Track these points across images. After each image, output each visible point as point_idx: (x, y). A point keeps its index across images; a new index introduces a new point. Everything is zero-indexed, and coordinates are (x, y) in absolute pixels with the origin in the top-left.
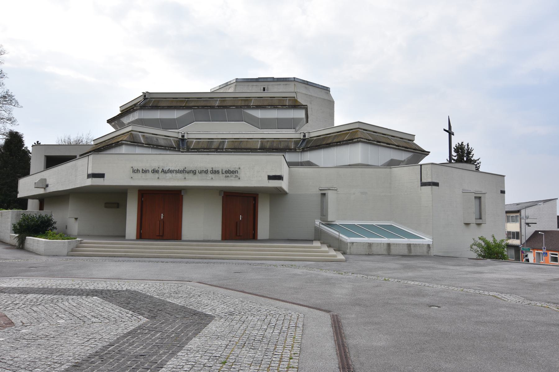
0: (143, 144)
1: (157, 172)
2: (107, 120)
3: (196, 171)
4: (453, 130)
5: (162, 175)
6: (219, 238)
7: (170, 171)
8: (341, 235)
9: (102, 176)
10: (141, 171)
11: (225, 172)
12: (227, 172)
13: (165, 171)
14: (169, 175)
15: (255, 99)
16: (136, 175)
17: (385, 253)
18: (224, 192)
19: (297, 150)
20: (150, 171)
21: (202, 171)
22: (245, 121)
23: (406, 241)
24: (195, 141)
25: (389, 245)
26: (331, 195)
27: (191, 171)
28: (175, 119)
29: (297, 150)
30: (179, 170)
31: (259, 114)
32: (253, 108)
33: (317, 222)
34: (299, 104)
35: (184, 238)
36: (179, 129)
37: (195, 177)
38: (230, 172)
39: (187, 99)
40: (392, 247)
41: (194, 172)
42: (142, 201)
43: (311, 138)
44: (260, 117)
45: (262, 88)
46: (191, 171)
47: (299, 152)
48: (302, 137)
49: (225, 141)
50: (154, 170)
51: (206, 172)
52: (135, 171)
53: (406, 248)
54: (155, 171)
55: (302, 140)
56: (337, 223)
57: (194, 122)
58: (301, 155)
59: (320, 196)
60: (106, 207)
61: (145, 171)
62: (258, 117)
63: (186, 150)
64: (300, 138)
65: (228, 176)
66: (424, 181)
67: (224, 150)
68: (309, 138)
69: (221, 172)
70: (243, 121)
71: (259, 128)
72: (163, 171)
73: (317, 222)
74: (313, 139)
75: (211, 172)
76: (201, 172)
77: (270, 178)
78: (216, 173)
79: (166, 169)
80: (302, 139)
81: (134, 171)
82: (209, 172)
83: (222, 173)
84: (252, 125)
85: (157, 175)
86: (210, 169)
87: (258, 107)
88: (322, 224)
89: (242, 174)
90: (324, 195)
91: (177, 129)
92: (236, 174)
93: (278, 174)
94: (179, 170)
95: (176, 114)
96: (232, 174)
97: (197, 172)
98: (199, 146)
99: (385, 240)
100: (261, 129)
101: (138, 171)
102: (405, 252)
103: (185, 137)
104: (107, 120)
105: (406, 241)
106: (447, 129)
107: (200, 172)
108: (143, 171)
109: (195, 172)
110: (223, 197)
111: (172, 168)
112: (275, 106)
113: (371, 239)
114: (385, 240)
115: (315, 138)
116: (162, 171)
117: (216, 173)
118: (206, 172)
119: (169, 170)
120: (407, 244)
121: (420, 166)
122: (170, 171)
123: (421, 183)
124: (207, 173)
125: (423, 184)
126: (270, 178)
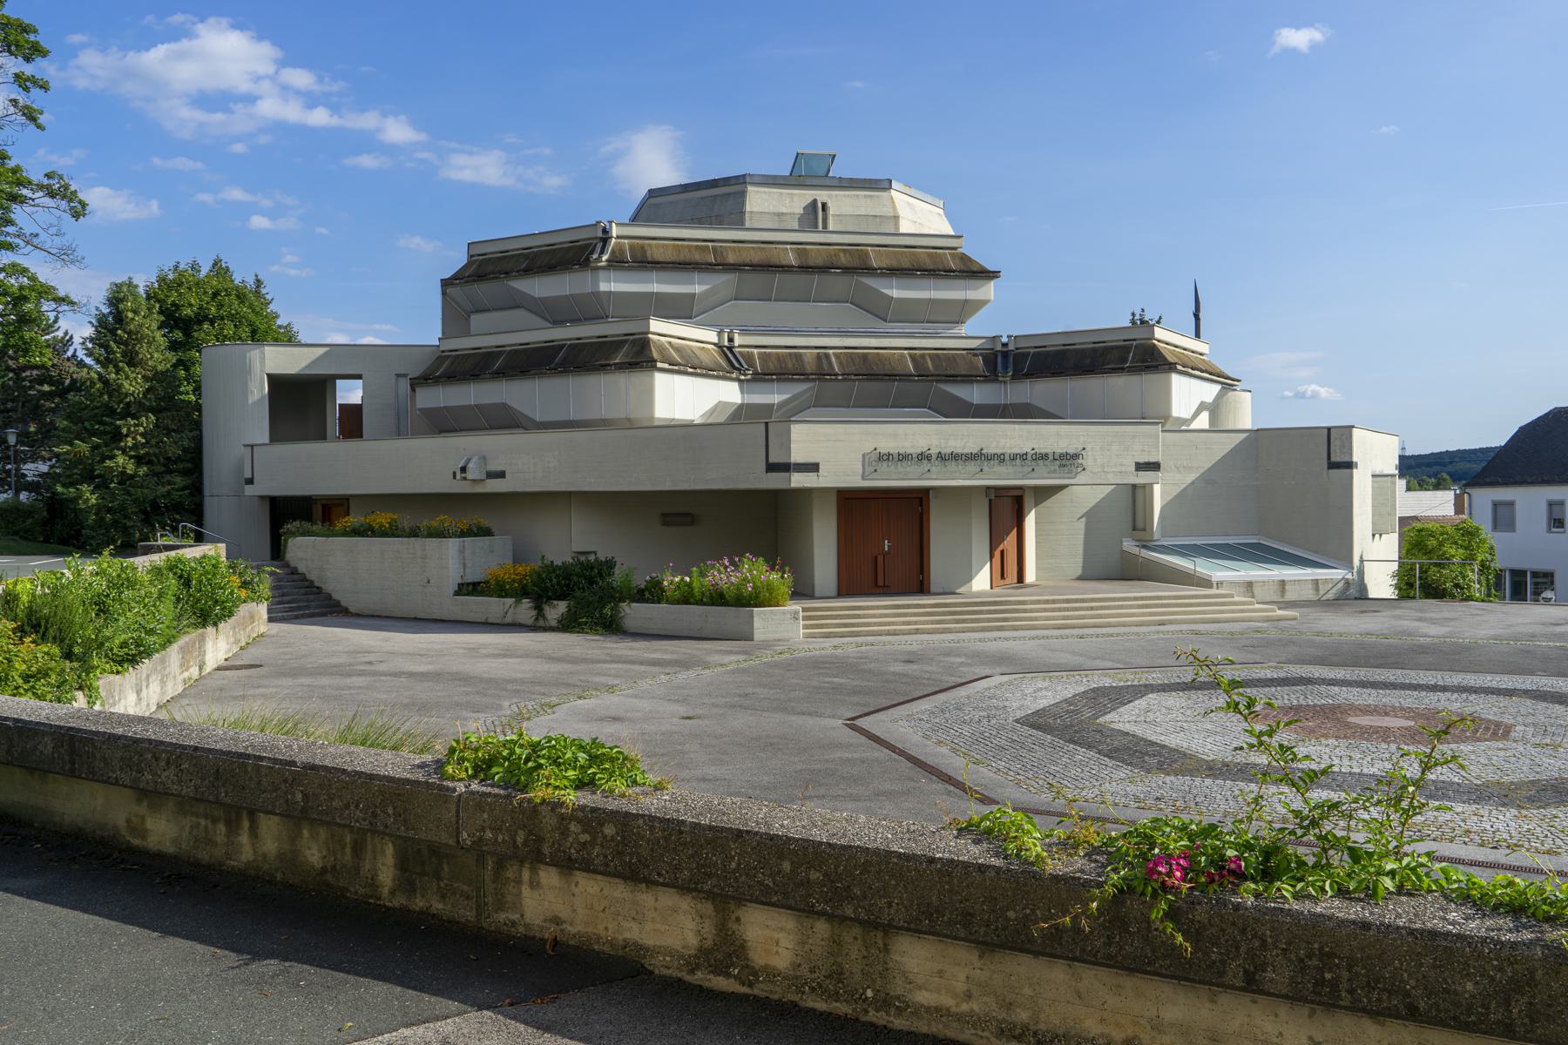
0: (679, 364)
1: (929, 458)
2: (442, 280)
5: (936, 468)
10: (896, 456)
14: (952, 466)
15: (875, 251)
16: (884, 467)
19: (1001, 379)
24: (759, 354)
25: (1283, 583)
29: (1001, 379)
32: (882, 275)
33: (1129, 545)
35: (933, 589)
37: (1002, 469)
39: (710, 244)
40: (1287, 587)
43: (1017, 349)
49: (827, 356)
52: (884, 458)
53: (1310, 586)
56: (1165, 543)
60: (665, 524)
63: (749, 377)
67: (840, 377)
69: (1051, 457)
71: (885, 320)
73: (1129, 545)
74: (1029, 353)
76: (1014, 457)
77: (1140, 467)
85: (926, 465)
87: (895, 272)
88: (1144, 547)
89: (1087, 461)
93: (1152, 459)
97: (1007, 457)
98: (772, 366)
102: (1309, 594)
104: (442, 280)
111: (959, 451)
112: (930, 271)
113: (1252, 573)
115: (1032, 351)
118: (1024, 456)
122: (955, 457)
126: (1140, 467)
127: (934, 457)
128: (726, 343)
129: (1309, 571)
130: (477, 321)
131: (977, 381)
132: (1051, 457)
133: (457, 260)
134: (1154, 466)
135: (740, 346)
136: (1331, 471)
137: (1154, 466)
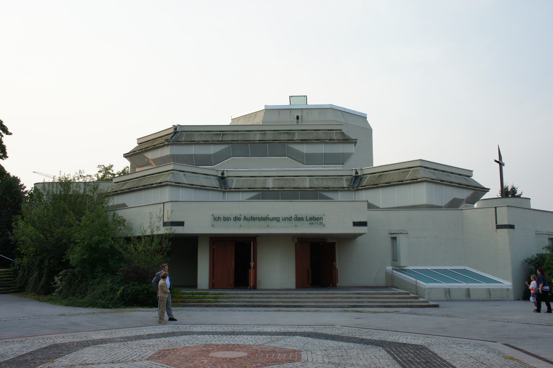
3: (279, 218)
4: (504, 161)
6: (294, 286)
7: (253, 219)
8: (418, 281)
9: (181, 224)
10: (222, 218)
11: (310, 219)
12: (311, 219)
13: (247, 218)
14: (252, 223)
16: (216, 223)
17: (465, 298)
18: (298, 238)
20: (232, 219)
21: (286, 218)
22: (287, 157)
23: (484, 285)
25: (468, 290)
26: (401, 239)
27: (275, 218)
28: (211, 155)
30: (262, 217)
31: (304, 149)
33: (389, 268)
34: (347, 138)
36: (214, 165)
38: (314, 219)
41: (277, 219)
42: (214, 249)
43: (364, 175)
44: (306, 152)
45: (296, 117)
46: (275, 218)
47: (352, 191)
48: (354, 174)
50: (236, 218)
51: (290, 219)
52: (217, 219)
54: (236, 219)
55: (355, 177)
57: (231, 157)
58: (355, 194)
59: (390, 240)
61: (226, 219)
62: (303, 151)
64: (352, 176)
65: (312, 223)
66: (499, 223)
68: (362, 175)
69: (305, 219)
70: (285, 156)
71: (304, 164)
72: (245, 218)
73: (389, 268)
75: (295, 219)
76: (285, 219)
77: (356, 224)
78: (300, 220)
79: (248, 216)
80: (354, 176)
81: (215, 219)
82: (293, 219)
83: (306, 220)
84: (295, 160)
86: (293, 216)
88: (395, 270)
90: (394, 239)
91: (212, 165)
92: (321, 221)
94: (262, 217)
95: (212, 150)
96: (316, 221)
99: (464, 285)
100: (306, 165)
101: (219, 218)
102: (485, 296)
103: (225, 175)
104: (124, 154)
105: (484, 285)
106: (498, 160)
107: (283, 219)
108: (225, 219)
109: (278, 219)
110: (296, 243)
112: (322, 140)
113: (449, 284)
114: (464, 285)
116: (244, 219)
117: (300, 220)
118: (290, 219)
119: (251, 217)
120: (487, 289)
121: (494, 208)
122: (253, 219)
123: (497, 226)
124: (291, 220)
125: (499, 227)
126: (356, 224)
127: (242, 218)
128: (220, 175)
129: (485, 284)
130: (137, 170)
131: (341, 191)
132: (305, 219)
133: (132, 145)
134: (364, 224)
135: (228, 177)
136: (498, 230)
137: (364, 224)
